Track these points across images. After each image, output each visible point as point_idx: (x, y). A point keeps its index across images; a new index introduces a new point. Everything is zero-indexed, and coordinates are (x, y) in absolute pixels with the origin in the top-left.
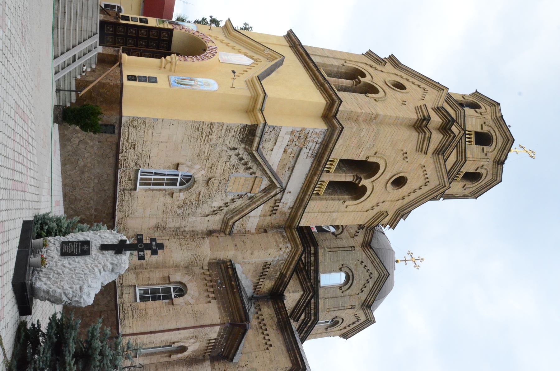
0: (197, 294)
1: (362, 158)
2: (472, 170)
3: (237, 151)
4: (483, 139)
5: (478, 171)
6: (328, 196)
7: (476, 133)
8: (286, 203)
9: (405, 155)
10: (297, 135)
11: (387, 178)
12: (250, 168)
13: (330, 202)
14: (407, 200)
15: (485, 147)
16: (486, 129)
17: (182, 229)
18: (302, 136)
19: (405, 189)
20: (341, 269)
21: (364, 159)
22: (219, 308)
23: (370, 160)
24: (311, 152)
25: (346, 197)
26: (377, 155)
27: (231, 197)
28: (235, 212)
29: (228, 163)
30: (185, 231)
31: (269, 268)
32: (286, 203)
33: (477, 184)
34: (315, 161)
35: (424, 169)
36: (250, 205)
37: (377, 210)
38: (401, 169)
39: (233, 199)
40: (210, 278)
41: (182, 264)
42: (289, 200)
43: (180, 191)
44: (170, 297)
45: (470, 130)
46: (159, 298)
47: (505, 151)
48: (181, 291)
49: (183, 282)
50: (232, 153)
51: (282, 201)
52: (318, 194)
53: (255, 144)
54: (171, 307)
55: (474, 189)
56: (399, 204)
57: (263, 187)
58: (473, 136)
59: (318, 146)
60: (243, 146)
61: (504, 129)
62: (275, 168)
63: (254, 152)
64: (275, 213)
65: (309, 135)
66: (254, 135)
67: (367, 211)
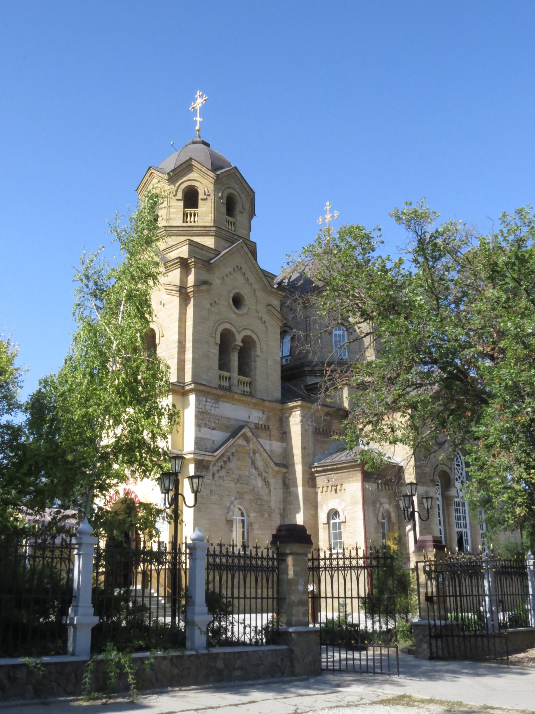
0: (338, 500)
1: (215, 350)
2: (224, 209)
3: (216, 472)
4: (191, 198)
5: (225, 202)
6: (253, 373)
7: (185, 206)
8: (259, 418)
9: (213, 304)
10: (200, 421)
11: (233, 316)
12: (229, 458)
13: (258, 371)
14: (256, 286)
15: (200, 197)
16: (180, 195)
17: (282, 511)
18: (201, 417)
19: (245, 292)
20: (330, 334)
21: (218, 347)
22: (349, 482)
23: (218, 341)
24: (214, 405)
25: (253, 353)
26: (213, 335)
27: (253, 471)
28: (267, 466)
29: (225, 478)
30: (284, 509)
31: (319, 429)
32: (259, 418)
33: (238, 197)
34: (222, 399)
35: (225, 277)
36: (261, 454)
37: (266, 318)
38: (226, 303)
39: (255, 468)
40: (325, 487)
41: (312, 512)
42: (256, 416)
43: (248, 516)
44: (340, 523)
45: (182, 216)
46: (340, 533)
47: (203, 170)
48: (333, 514)
49: (327, 511)
50: (216, 477)
51: (257, 422)
52: (250, 383)
53: (210, 459)
54: (347, 523)
55: (243, 197)
56: (259, 294)
57: (244, 443)
58: (188, 210)
59: (209, 400)
60: (211, 468)
61: (179, 170)
62: (228, 435)
63: (216, 458)
64: (268, 427)
65: (200, 410)
66: (203, 460)
67: (267, 328)
